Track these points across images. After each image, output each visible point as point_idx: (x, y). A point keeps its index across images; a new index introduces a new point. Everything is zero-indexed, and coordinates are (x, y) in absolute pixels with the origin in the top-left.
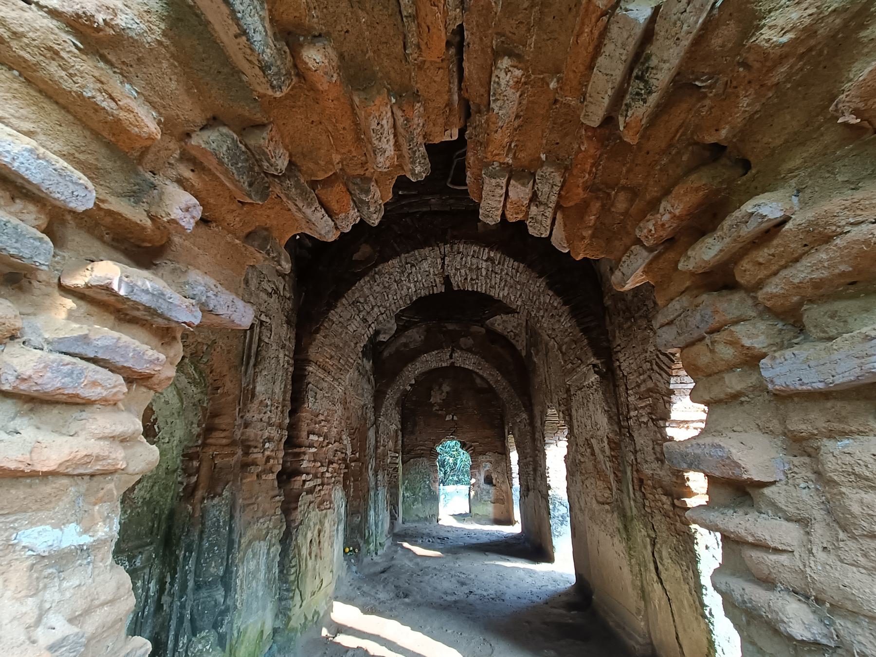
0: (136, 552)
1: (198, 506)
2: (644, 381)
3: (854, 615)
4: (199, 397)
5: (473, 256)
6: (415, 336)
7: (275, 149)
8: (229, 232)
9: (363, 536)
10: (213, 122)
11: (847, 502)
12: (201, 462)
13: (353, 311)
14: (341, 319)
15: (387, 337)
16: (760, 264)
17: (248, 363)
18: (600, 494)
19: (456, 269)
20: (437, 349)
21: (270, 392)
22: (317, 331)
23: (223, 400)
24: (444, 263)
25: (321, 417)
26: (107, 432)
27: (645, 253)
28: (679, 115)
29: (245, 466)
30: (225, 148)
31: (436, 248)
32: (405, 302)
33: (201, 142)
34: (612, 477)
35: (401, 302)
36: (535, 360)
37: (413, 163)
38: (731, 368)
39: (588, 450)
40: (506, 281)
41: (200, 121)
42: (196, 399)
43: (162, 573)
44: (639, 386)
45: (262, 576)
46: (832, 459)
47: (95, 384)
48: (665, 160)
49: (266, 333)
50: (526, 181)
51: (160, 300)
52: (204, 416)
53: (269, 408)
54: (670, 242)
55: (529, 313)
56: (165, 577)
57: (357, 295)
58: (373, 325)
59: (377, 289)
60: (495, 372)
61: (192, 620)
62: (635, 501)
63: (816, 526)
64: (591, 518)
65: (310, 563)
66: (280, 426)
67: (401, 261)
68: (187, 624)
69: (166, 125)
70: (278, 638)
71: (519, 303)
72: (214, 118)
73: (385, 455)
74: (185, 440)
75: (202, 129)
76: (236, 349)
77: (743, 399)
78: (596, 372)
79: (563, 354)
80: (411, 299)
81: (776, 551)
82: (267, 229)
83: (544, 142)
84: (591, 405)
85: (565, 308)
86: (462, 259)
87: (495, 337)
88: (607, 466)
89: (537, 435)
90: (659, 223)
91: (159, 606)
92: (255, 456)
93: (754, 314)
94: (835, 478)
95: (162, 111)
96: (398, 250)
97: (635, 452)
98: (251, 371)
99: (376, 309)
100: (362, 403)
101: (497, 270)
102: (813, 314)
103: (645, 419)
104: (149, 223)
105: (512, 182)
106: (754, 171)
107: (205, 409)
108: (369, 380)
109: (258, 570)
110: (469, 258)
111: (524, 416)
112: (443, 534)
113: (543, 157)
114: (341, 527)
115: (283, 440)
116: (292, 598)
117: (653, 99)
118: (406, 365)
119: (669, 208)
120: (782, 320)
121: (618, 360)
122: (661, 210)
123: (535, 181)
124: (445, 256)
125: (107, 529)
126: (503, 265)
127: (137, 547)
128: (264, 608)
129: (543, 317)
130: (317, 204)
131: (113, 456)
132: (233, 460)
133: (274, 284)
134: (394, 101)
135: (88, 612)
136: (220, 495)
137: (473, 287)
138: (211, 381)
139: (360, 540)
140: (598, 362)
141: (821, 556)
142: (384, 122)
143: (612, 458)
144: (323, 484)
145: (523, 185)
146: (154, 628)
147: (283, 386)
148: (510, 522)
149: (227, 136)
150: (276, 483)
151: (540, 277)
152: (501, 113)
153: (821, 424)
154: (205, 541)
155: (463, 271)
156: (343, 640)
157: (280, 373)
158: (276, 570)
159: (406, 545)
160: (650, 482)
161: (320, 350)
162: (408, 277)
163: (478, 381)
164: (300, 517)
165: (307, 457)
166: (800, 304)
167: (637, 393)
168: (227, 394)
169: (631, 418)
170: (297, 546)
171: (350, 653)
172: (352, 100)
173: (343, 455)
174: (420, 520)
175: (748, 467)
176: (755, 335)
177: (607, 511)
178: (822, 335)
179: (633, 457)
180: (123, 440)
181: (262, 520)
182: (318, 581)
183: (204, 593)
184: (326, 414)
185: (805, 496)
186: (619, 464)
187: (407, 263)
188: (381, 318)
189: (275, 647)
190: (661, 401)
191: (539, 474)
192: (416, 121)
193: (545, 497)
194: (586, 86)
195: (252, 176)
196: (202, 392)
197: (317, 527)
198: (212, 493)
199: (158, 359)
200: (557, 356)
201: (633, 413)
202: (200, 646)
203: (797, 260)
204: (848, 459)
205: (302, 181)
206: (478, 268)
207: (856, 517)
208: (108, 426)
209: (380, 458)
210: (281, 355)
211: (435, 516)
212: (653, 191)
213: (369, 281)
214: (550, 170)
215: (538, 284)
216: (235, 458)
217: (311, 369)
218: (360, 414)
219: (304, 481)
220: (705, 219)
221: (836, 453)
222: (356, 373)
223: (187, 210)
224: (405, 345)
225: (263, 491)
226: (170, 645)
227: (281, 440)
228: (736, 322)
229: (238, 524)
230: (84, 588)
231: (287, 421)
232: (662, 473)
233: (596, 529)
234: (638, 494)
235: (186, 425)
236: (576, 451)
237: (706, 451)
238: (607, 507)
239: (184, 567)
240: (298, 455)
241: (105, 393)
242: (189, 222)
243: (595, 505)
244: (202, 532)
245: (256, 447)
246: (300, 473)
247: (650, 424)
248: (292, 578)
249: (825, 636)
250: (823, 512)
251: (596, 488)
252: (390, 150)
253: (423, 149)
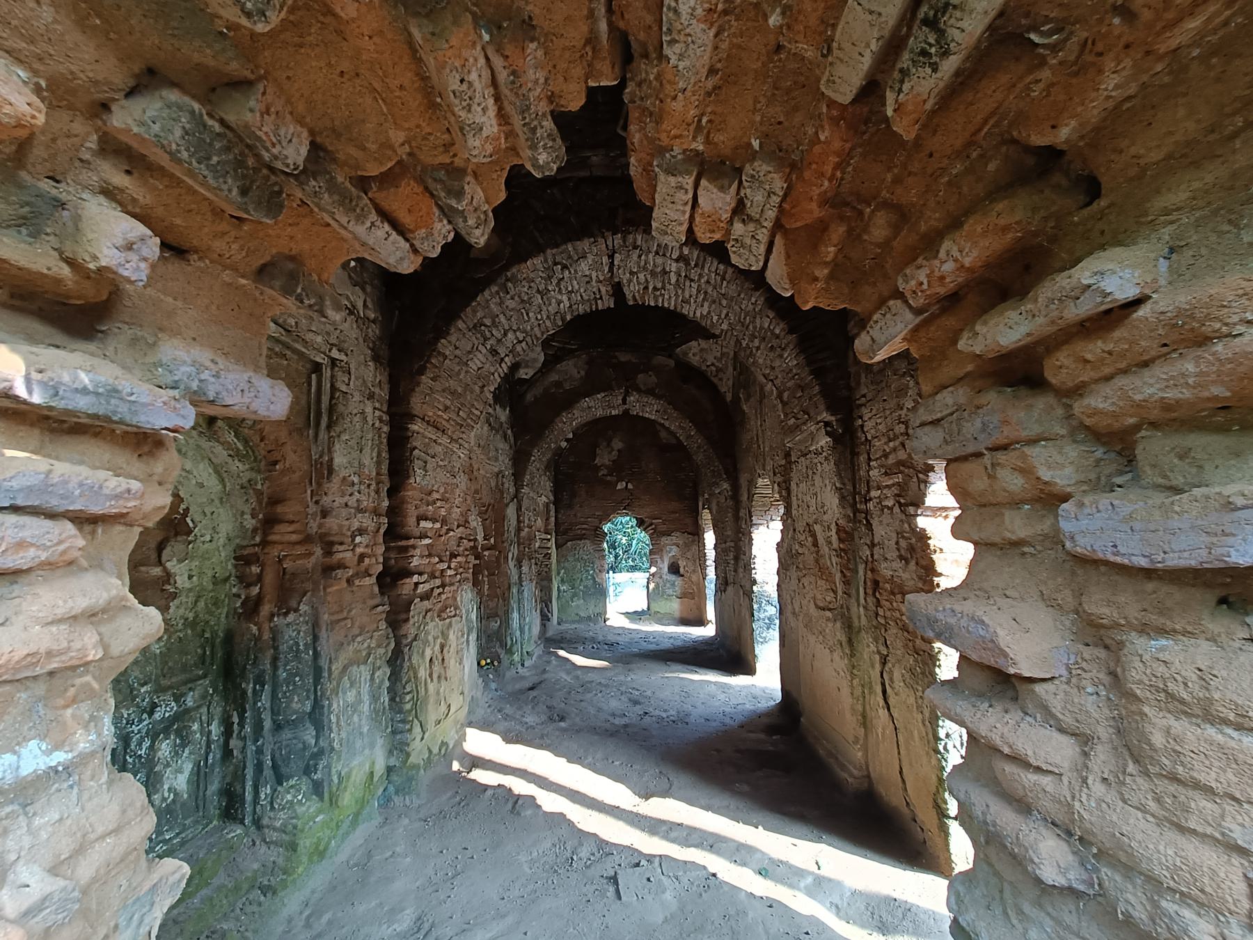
0: (183, 689)
1: (266, 626)
2: (895, 449)
3: (1130, 869)
4: (248, 475)
5: (657, 253)
6: (572, 370)
7: (277, 127)
8: (225, 267)
9: (503, 645)
10: (148, 79)
11: (1148, 728)
12: (263, 566)
13: (475, 339)
14: (457, 352)
15: (531, 372)
16: (1087, 361)
17: (318, 424)
18: (820, 597)
19: (632, 273)
20: (604, 391)
21: (356, 464)
22: (422, 371)
23: (286, 479)
24: (612, 264)
25: (436, 496)
26: (60, 612)
27: (909, 316)
28: (992, 95)
29: (328, 570)
30: (178, 133)
31: (601, 240)
32: (554, 323)
33: (130, 121)
34: (838, 575)
35: (548, 323)
36: (745, 407)
37: (533, 147)
38: (1015, 504)
39: (810, 539)
40: (706, 293)
41: (121, 78)
42: (244, 480)
43: (225, 711)
44: (886, 456)
45: (366, 707)
46: (1138, 664)
47: (21, 545)
48: (958, 168)
49: (339, 374)
50: (726, 182)
51: (113, 401)
52: (260, 502)
53: (356, 487)
54: (952, 301)
55: (738, 342)
56: (230, 717)
57: (479, 315)
58: (507, 359)
59: (511, 304)
60: (687, 424)
61: (275, 767)
62: (865, 608)
63: (1099, 748)
64: (806, 626)
65: (431, 687)
66: (376, 512)
67: (546, 261)
68: (268, 772)
69: (56, 92)
70: (394, 778)
71: (725, 327)
72: (151, 71)
73: (531, 538)
74: (237, 537)
75: (130, 93)
77: (1026, 549)
78: (828, 434)
79: (784, 404)
80: (563, 319)
81: (1038, 769)
82: (292, 258)
83: (758, 118)
84: (817, 478)
85: (790, 337)
86: (640, 256)
87: (691, 374)
88: (833, 562)
89: (742, 513)
90: (937, 274)
91: (227, 753)
92: (341, 555)
93: (1063, 432)
94: (1138, 692)
95: (36, 65)
96: (541, 241)
97: (872, 546)
98: (323, 435)
99: (510, 335)
100: (496, 470)
101: (694, 274)
102: (1152, 447)
103: (890, 503)
104: (66, 271)
105: (704, 182)
106: (1103, 202)
107: (259, 494)
108: (505, 437)
109: (359, 701)
110: (651, 256)
111: (726, 486)
112: (611, 638)
113: (756, 144)
114: (473, 637)
115: (382, 531)
116: (410, 730)
117: (949, 65)
118: (558, 414)
119: (956, 254)
120: (1104, 444)
121: (861, 417)
122: (942, 254)
123: (740, 182)
124: (615, 252)
125: (93, 737)
126: (703, 267)
127: (185, 683)
128: (372, 746)
129: (758, 348)
130: (373, 216)
131: (77, 645)
132: (310, 563)
133: (348, 298)
134: (487, 37)
135: (80, 851)
136: (296, 610)
137: (656, 301)
138: (263, 452)
139: (499, 651)
140: (833, 418)
141: (1098, 789)
142: (473, 76)
143: (840, 552)
144: (443, 586)
145: (722, 189)
146: (224, 777)
147: (375, 455)
148: (700, 622)
149: (180, 108)
150: (376, 589)
151: (756, 289)
152: (681, 65)
153: (1133, 613)
154: (280, 671)
155: (641, 276)
156: (479, 775)
157: (370, 436)
158: (385, 698)
159: (562, 653)
160: (888, 586)
161: (428, 399)
162: (558, 284)
163: (663, 434)
164: (413, 631)
165: (418, 552)
166: (1137, 428)
167: (882, 466)
168: (290, 470)
169: (871, 499)
170: (411, 667)
171: (489, 792)
172: (410, 34)
173: (472, 544)
174: (581, 620)
175: (1017, 658)
176: (1059, 465)
177: (828, 619)
178: (1161, 481)
179: (868, 553)
180: (92, 616)
181: (359, 639)
182: (443, 708)
183: (286, 734)
184: (442, 490)
185: (1092, 706)
186: (849, 560)
187: (556, 264)
188: (519, 348)
189: (391, 789)
190: (915, 479)
191: (741, 564)
192: (531, 75)
193: (749, 594)
194: (834, 26)
195: (244, 177)
196: (252, 469)
197: (439, 641)
198: (284, 607)
199: (129, 491)
200: (775, 406)
201: (874, 493)
202: (289, 797)
203: (1145, 364)
204: (1161, 669)
205: (340, 179)
206: (664, 272)
207: (1155, 751)
208: (61, 603)
209: (524, 543)
210: (369, 410)
211: (601, 615)
212: (933, 219)
213: (497, 293)
214: (765, 168)
215: (753, 300)
216: (313, 559)
217: (415, 427)
218: (493, 484)
219: (417, 584)
220: (1007, 280)
221: (1146, 657)
222: (486, 428)
223: (129, 247)
224: (558, 384)
225: (358, 600)
226: (249, 797)
227: (378, 531)
228: (1033, 442)
229: (325, 646)
230: (69, 822)
231: (386, 503)
232: (905, 576)
233: (812, 639)
234: (870, 600)
235: (235, 515)
236: (793, 538)
237: (963, 623)
238: (828, 614)
239: (255, 703)
240: (405, 549)
241: (44, 556)
242: (138, 269)
243: (813, 611)
244: (275, 659)
245: (341, 544)
246: (410, 574)
247: (897, 509)
248: (408, 706)
249: (1084, 882)
250: (1111, 730)
251: (816, 590)
252: (490, 124)
253: (549, 124)
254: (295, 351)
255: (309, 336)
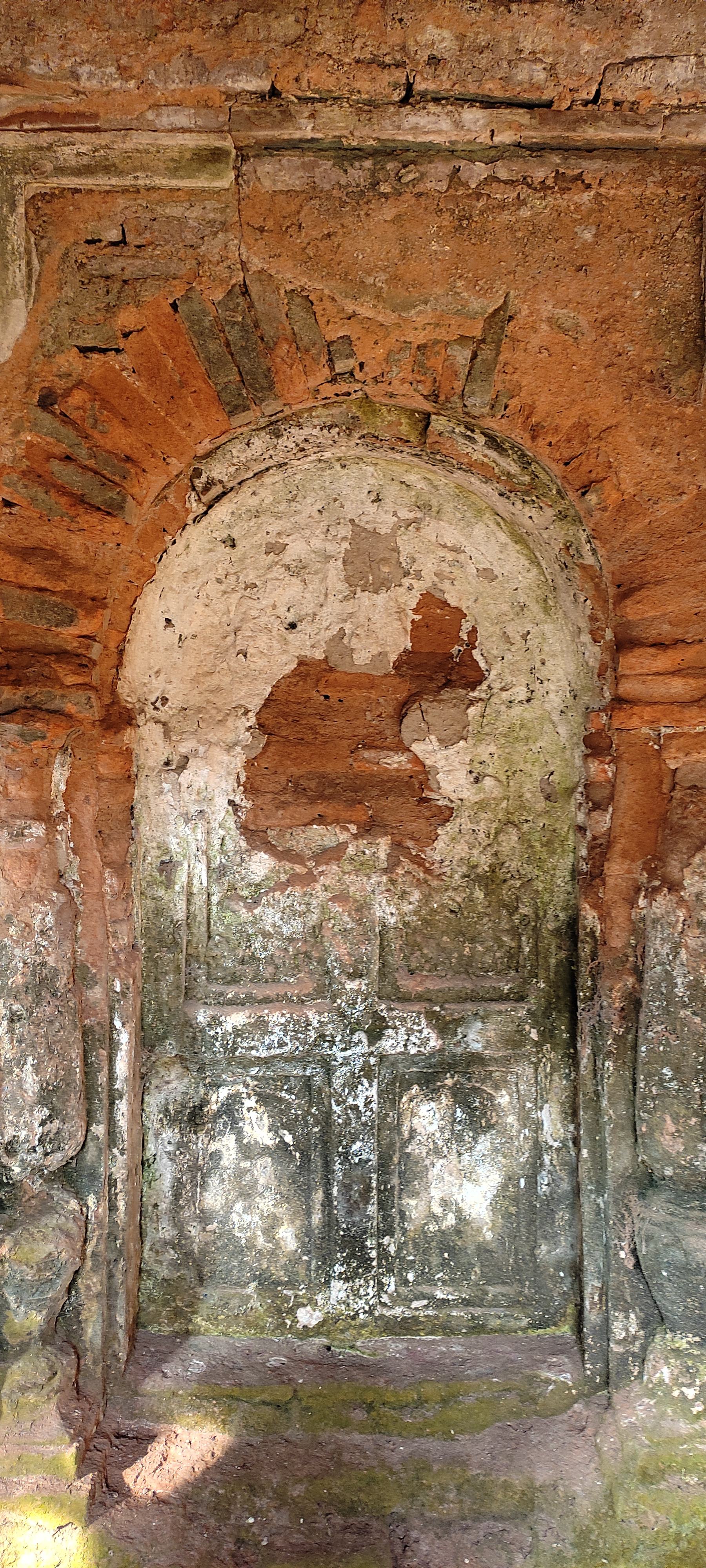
1: (619, 913)
76: (653, 299)
127: (473, 997)
254: (613, 151)
255: (627, 86)
